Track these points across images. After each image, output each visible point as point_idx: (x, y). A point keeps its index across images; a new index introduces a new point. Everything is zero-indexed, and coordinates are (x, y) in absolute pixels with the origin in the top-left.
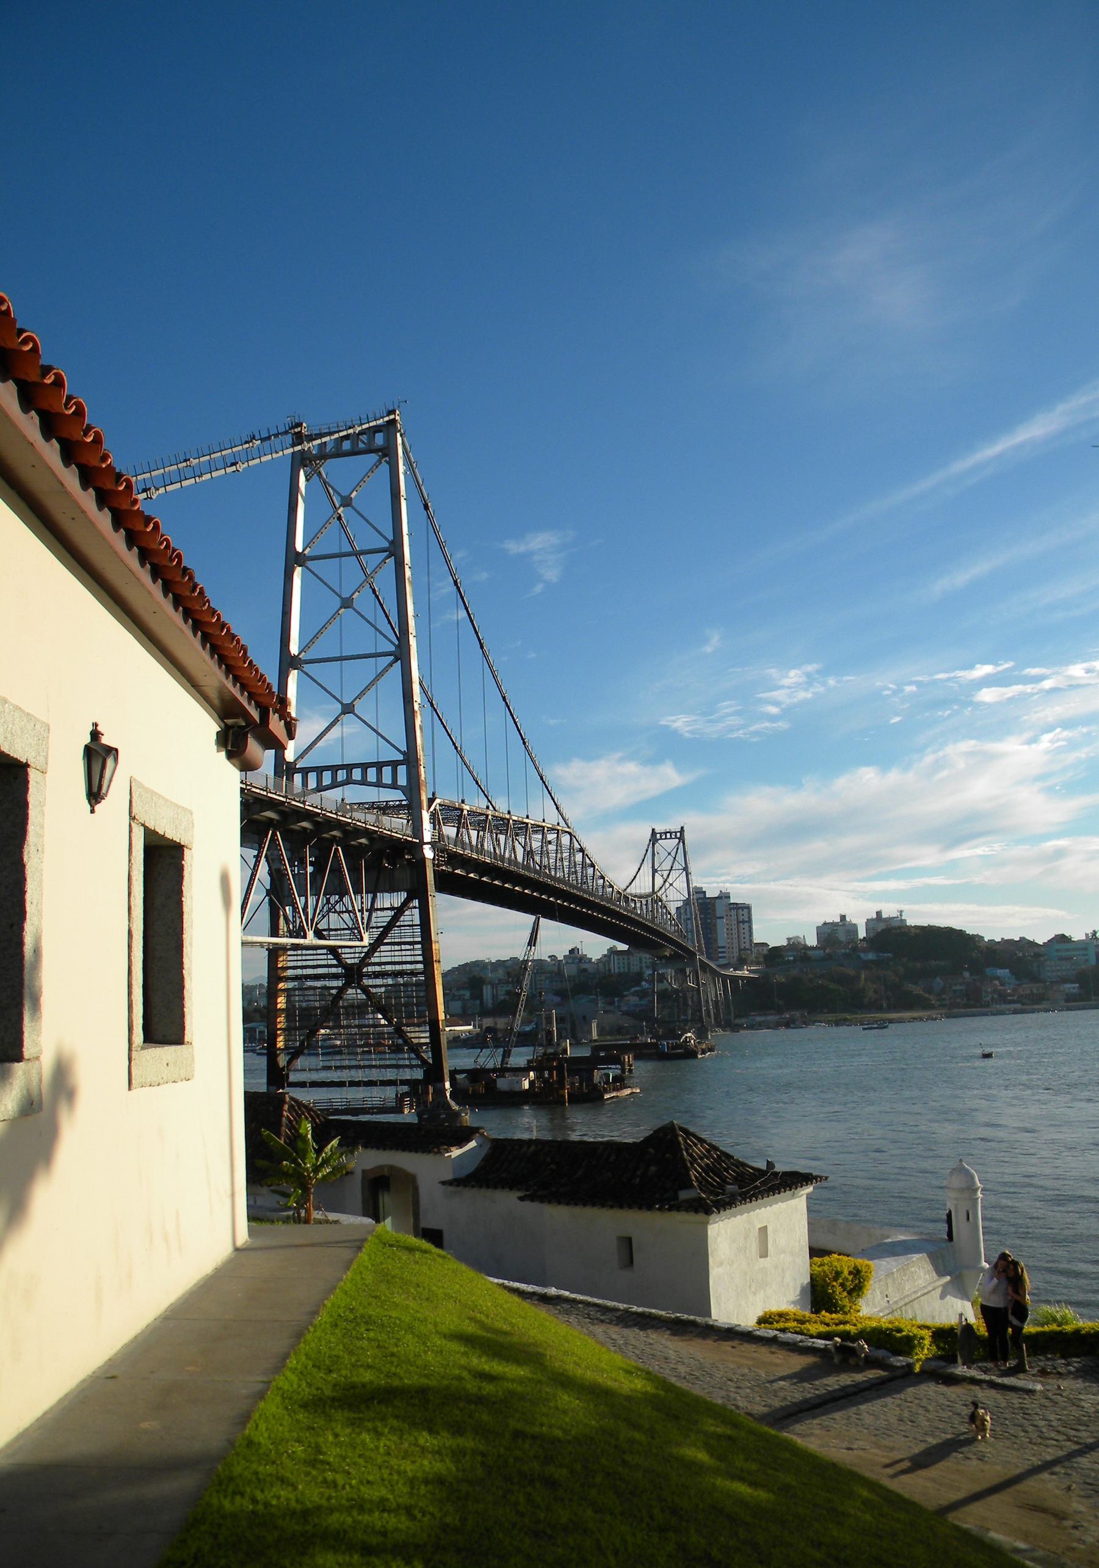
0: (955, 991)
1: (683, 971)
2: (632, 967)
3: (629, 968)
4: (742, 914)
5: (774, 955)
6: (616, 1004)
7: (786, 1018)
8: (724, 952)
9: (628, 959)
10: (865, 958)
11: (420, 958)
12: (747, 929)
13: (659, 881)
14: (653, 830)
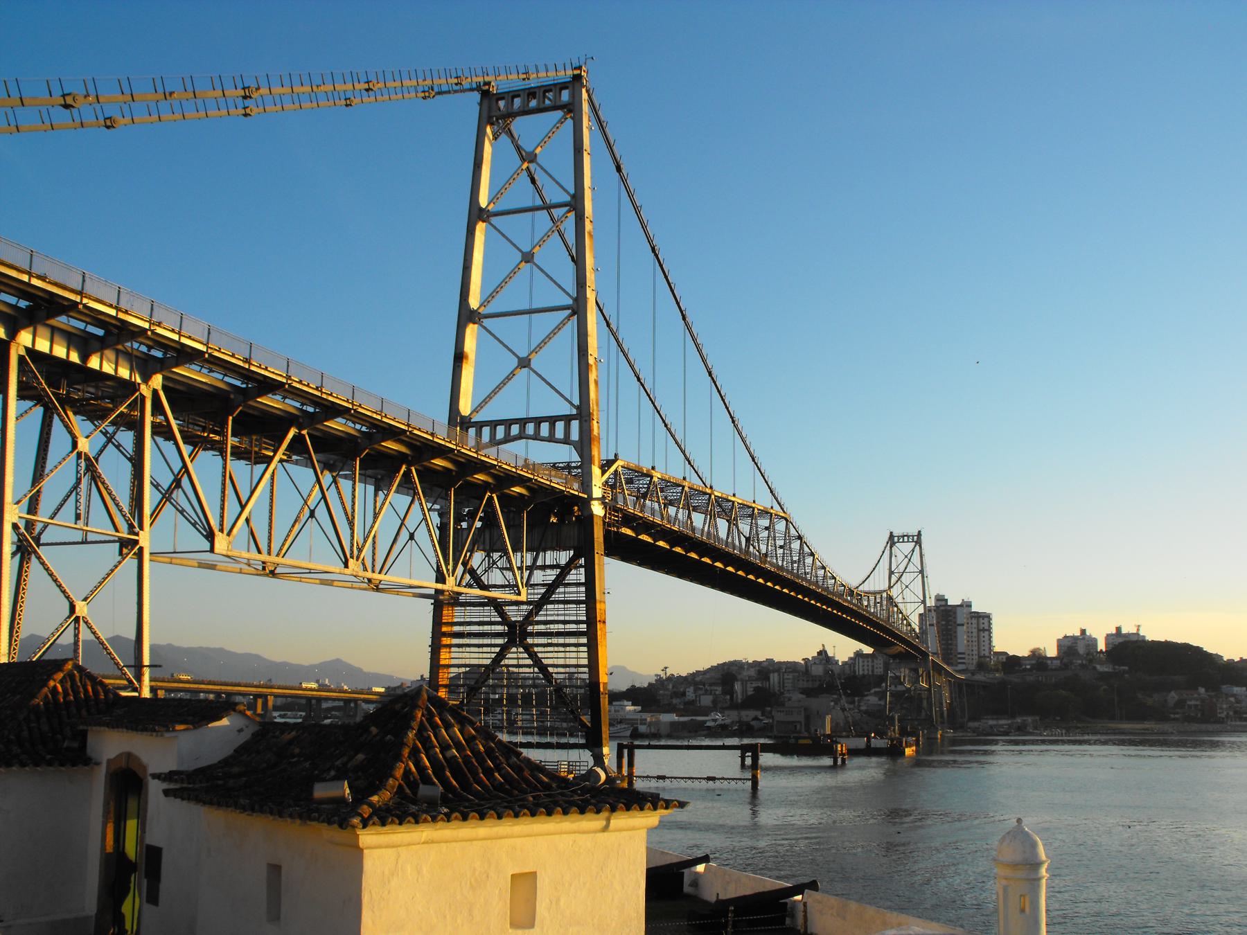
0: (1190, 706)
1: (916, 671)
2: (876, 670)
3: (873, 671)
4: (982, 622)
5: (1012, 662)
6: (857, 704)
7: (1017, 722)
8: (964, 658)
9: (873, 662)
10: (1101, 670)
11: (585, 618)
12: (987, 637)
13: (894, 579)
14: (891, 533)
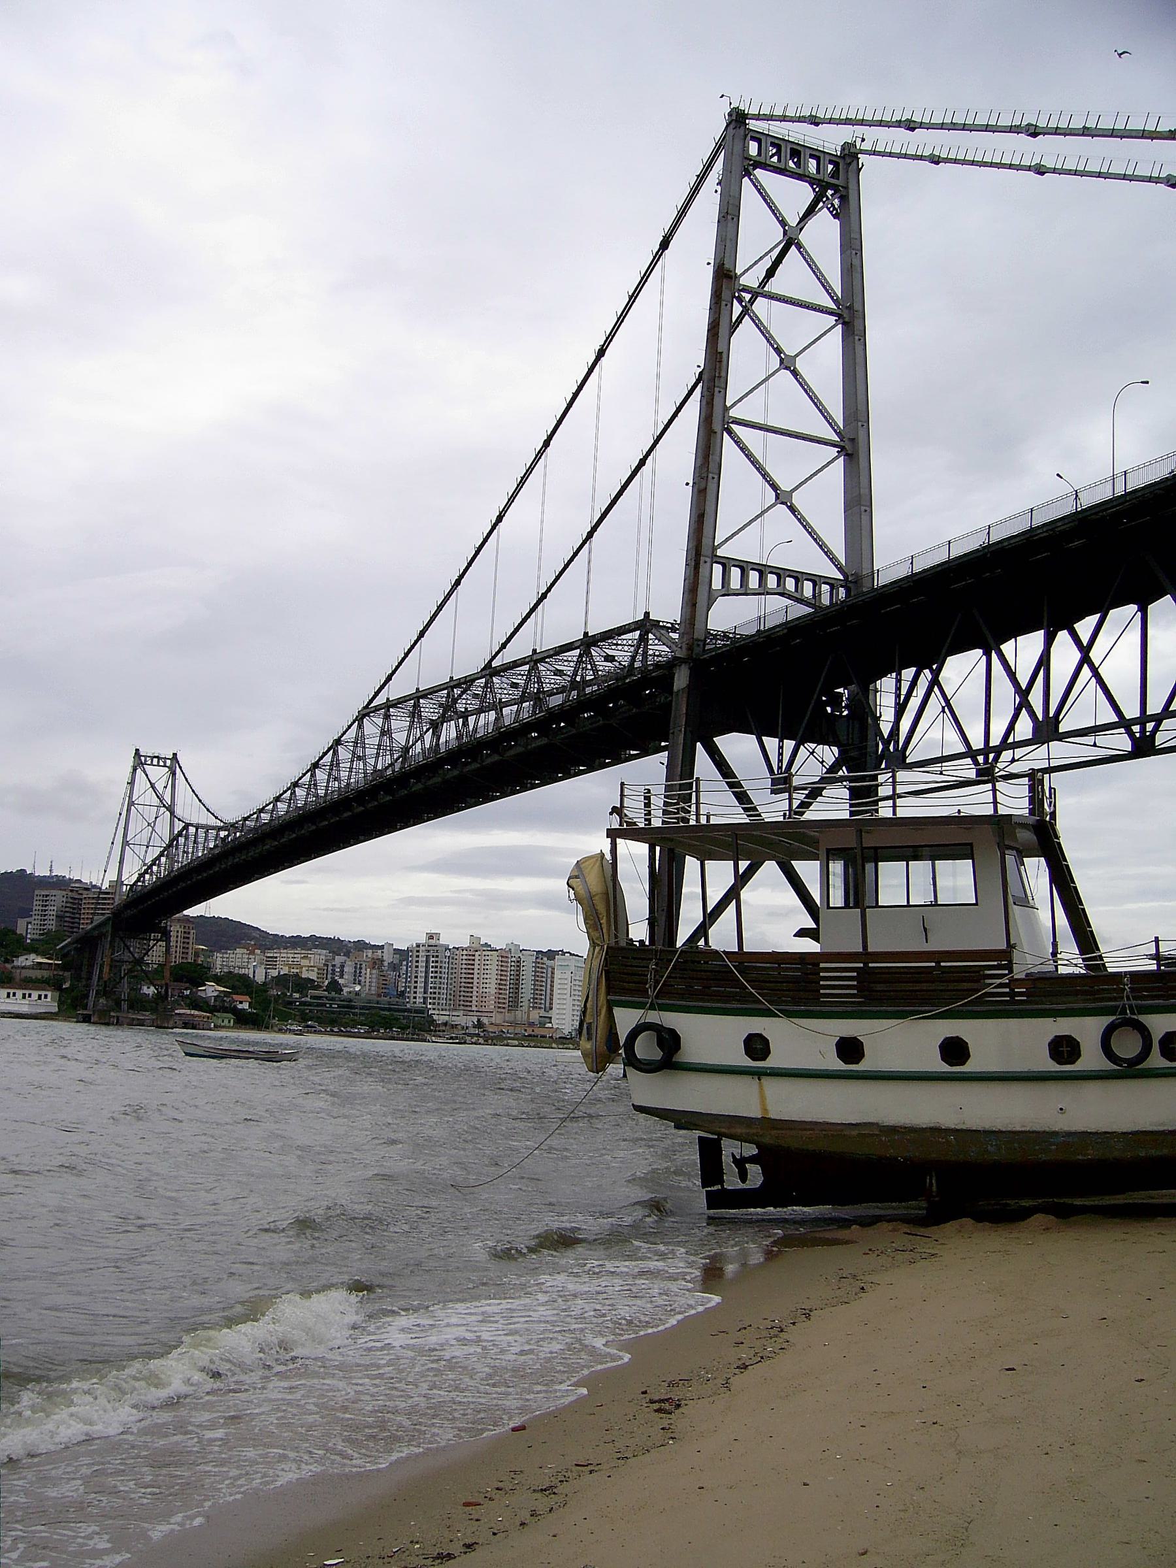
14: (137, 750)
